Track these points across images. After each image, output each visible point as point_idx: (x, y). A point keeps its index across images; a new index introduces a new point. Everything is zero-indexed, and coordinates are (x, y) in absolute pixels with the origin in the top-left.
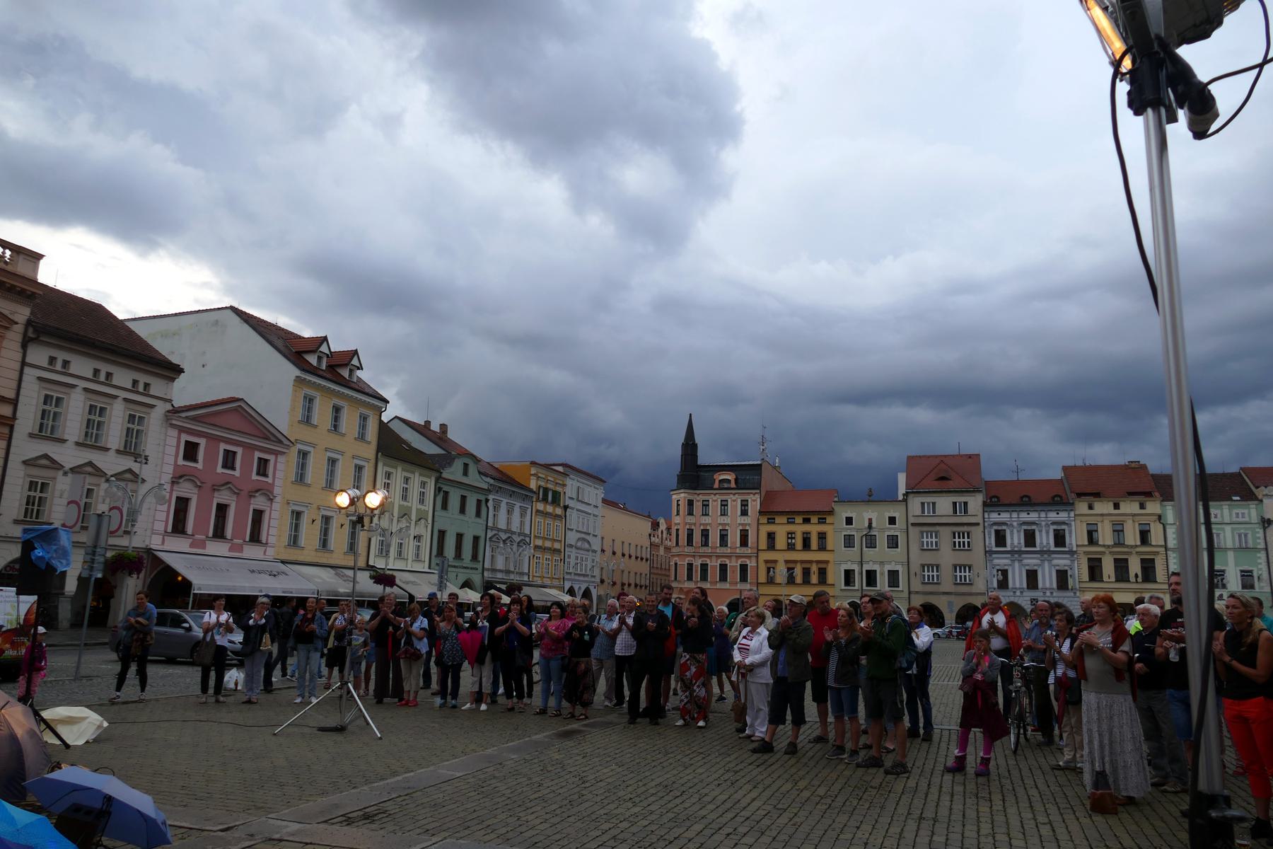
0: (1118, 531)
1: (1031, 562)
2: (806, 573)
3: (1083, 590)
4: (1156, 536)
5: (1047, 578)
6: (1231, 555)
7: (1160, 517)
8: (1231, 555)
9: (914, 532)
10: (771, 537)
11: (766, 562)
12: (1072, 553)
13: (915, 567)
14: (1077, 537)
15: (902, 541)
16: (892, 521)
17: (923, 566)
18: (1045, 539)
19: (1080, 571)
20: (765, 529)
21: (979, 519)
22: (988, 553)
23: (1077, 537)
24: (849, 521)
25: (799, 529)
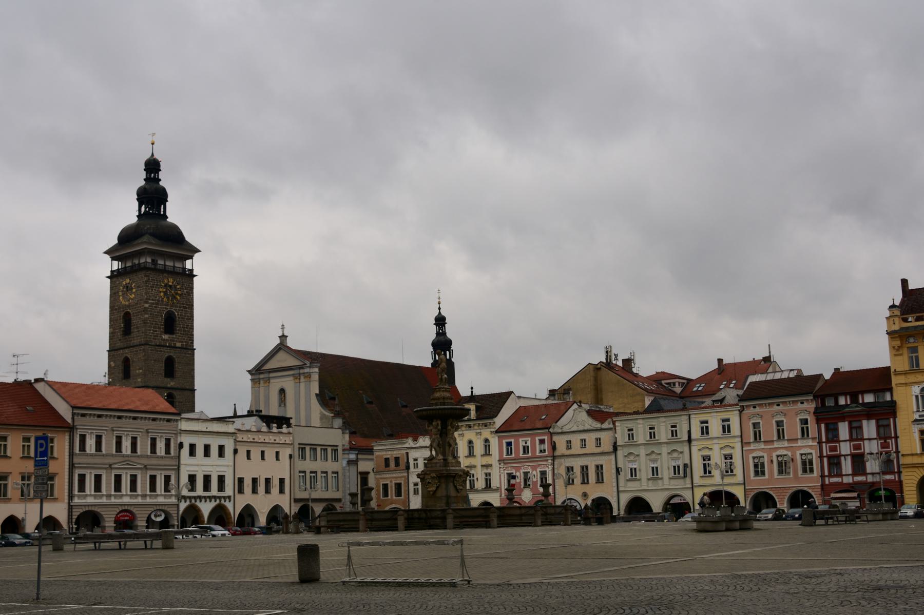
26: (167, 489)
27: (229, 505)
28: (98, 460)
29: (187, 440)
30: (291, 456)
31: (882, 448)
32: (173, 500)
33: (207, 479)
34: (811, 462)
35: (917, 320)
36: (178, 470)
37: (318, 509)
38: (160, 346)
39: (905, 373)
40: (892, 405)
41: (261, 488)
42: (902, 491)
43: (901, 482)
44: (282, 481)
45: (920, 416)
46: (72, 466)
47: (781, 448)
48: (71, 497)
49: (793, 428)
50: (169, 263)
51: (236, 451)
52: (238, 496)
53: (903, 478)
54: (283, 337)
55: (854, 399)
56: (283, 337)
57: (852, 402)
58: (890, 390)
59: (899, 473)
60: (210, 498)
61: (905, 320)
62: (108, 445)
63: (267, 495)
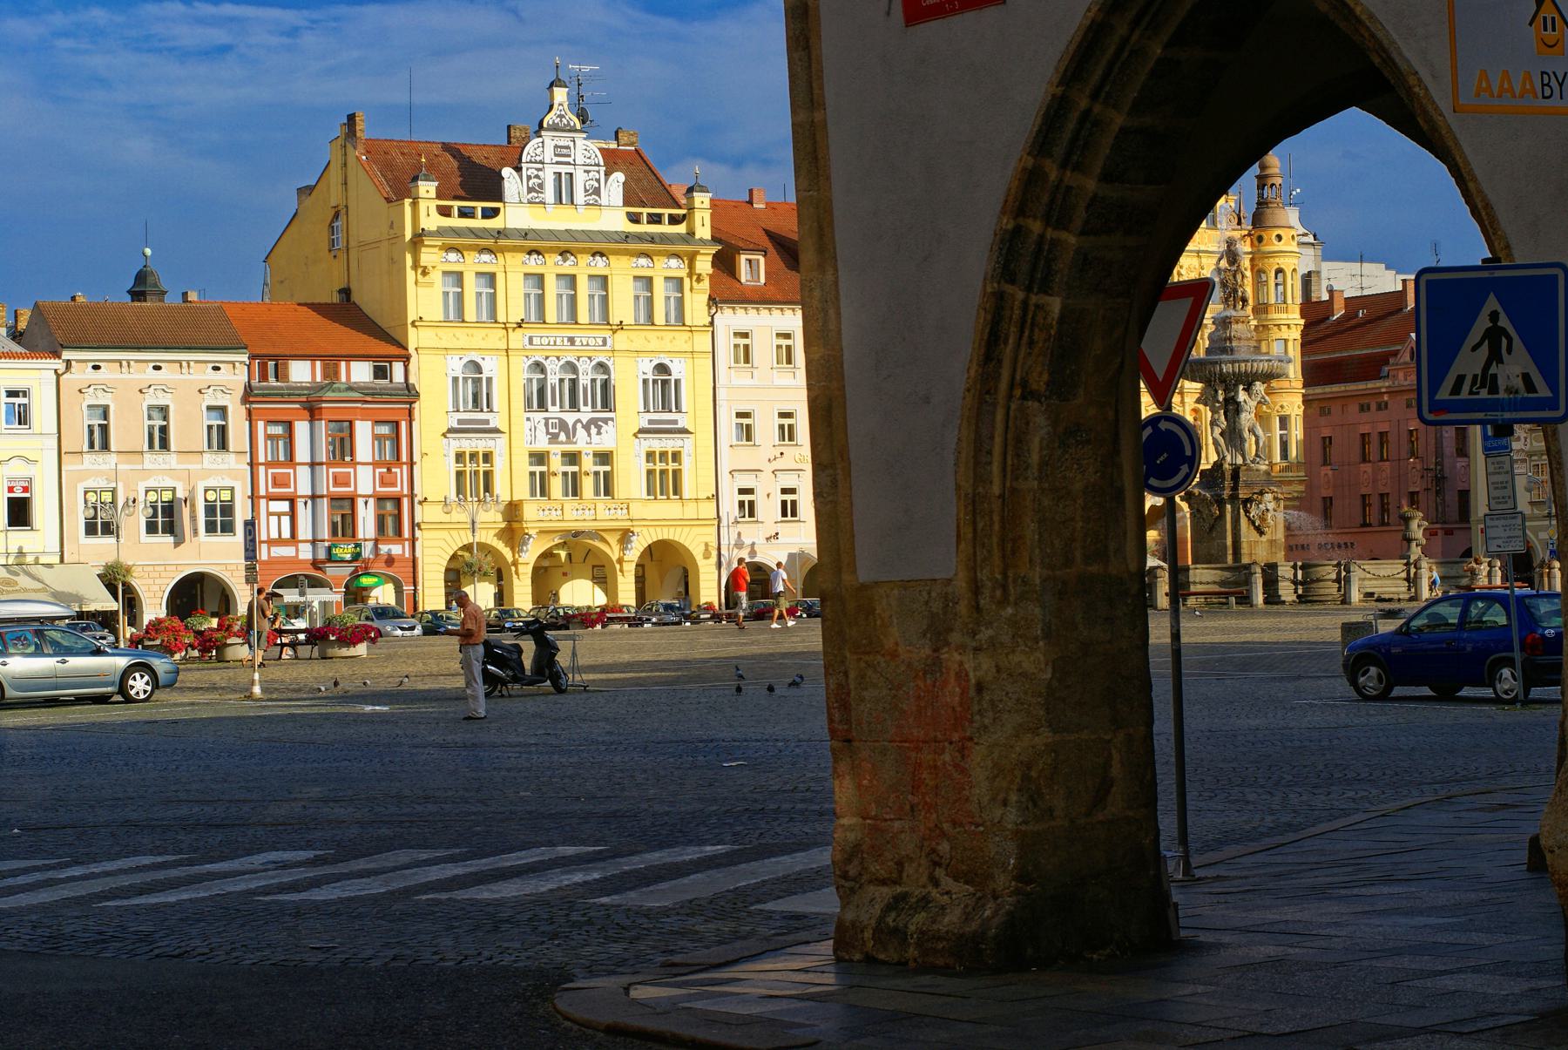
31: (383, 484)
34: (228, 509)
35: (464, 214)
39: (435, 325)
40: (410, 394)
42: (415, 584)
43: (414, 561)
45: (460, 422)
47: (163, 474)
49: (188, 428)
53: (418, 554)
55: (331, 373)
57: (325, 375)
58: (406, 359)
59: (413, 540)
61: (445, 212)
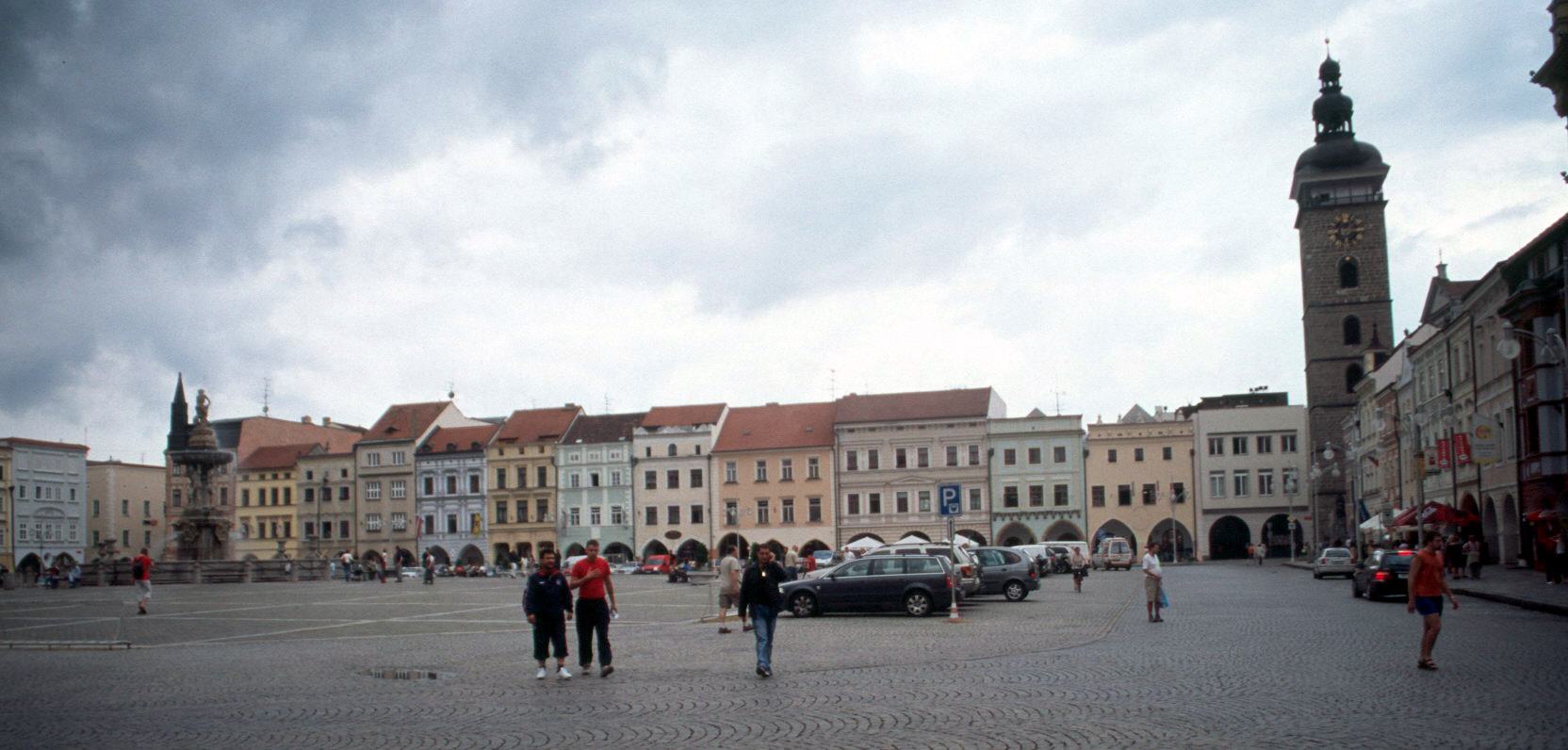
0: (522, 474)
1: (452, 507)
2: (274, 526)
3: (491, 532)
4: (550, 482)
5: (464, 523)
6: (605, 493)
7: (553, 460)
8: (605, 493)
9: (361, 482)
10: (246, 493)
11: (242, 518)
12: (483, 497)
13: (361, 517)
14: (488, 481)
15: (351, 493)
16: (345, 473)
17: (368, 516)
18: (464, 485)
19: (488, 514)
20: (240, 487)
21: (411, 469)
22: (419, 500)
23: (488, 481)
24: (310, 475)
25: (269, 485)
26: (975, 506)
27: (1078, 523)
28: (876, 477)
29: (1000, 448)
30: (1192, 453)
32: (984, 518)
33: (1036, 493)
36: (989, 479)
37: (1255, 525)
38: (1333, 305)
41: (1137, 498)
44: (1178, 489)
46: (839, 487)
48: (839, 518)
50: (1342, 195)
51: (1086, 454)
52: (1092, 511)
54: (1441, 267)
56: (1441, 267)
60: (1045, 514)
62: (888, 459)
63: (1150, 507)
